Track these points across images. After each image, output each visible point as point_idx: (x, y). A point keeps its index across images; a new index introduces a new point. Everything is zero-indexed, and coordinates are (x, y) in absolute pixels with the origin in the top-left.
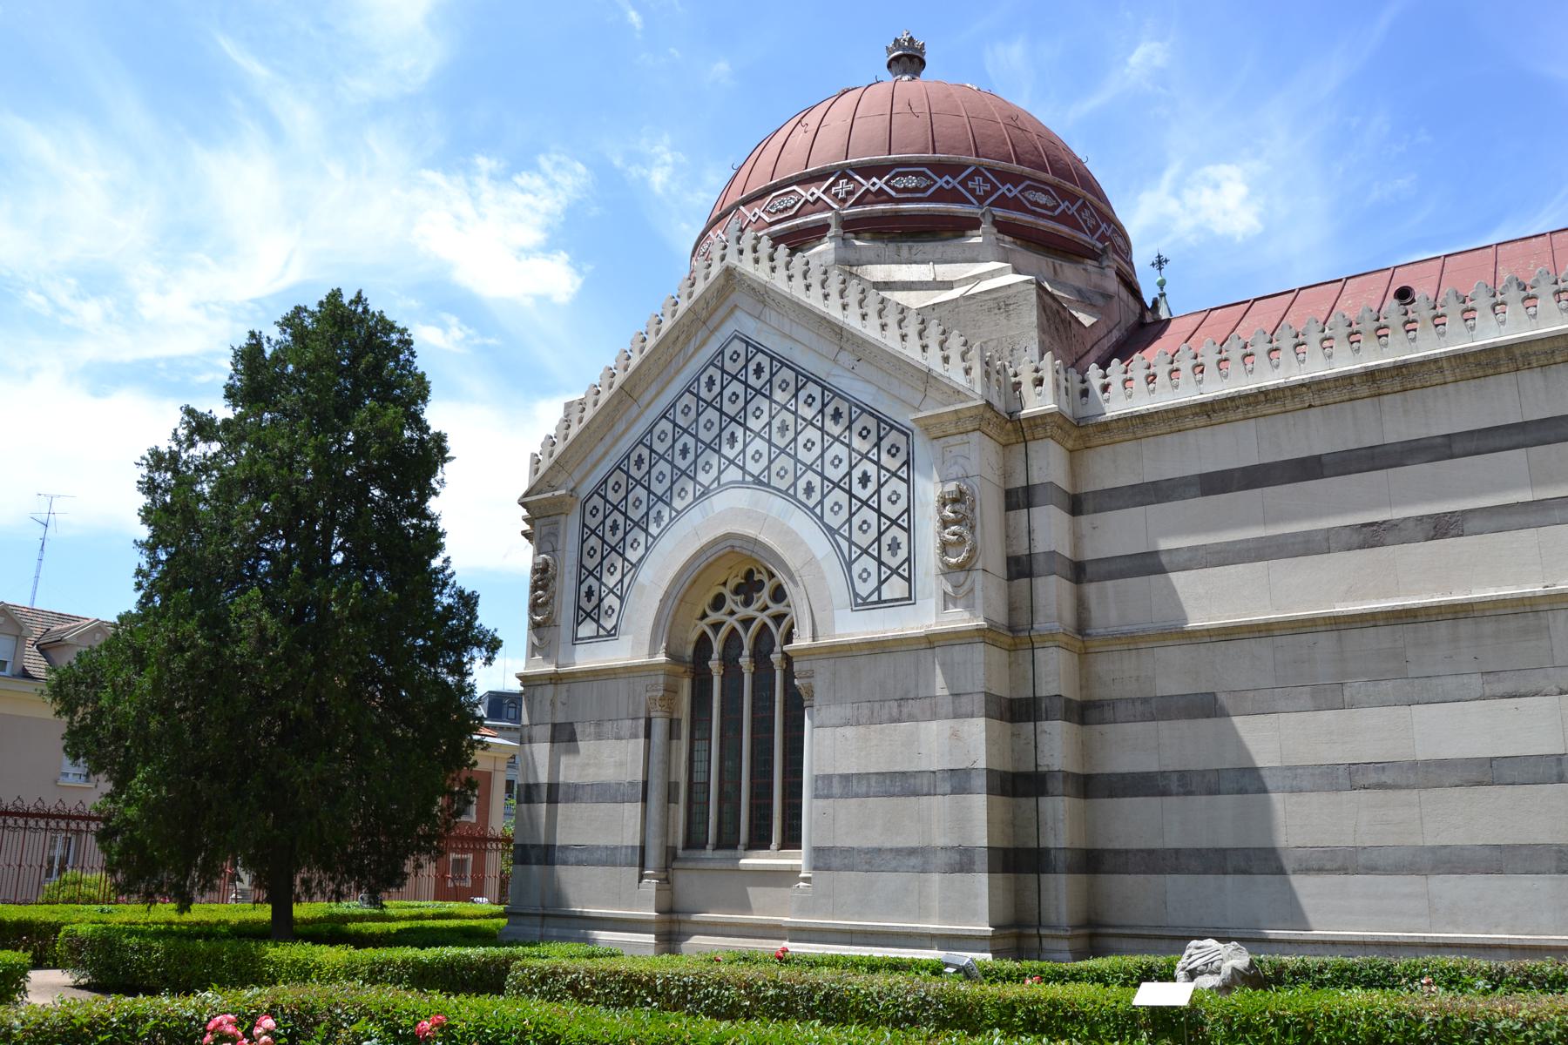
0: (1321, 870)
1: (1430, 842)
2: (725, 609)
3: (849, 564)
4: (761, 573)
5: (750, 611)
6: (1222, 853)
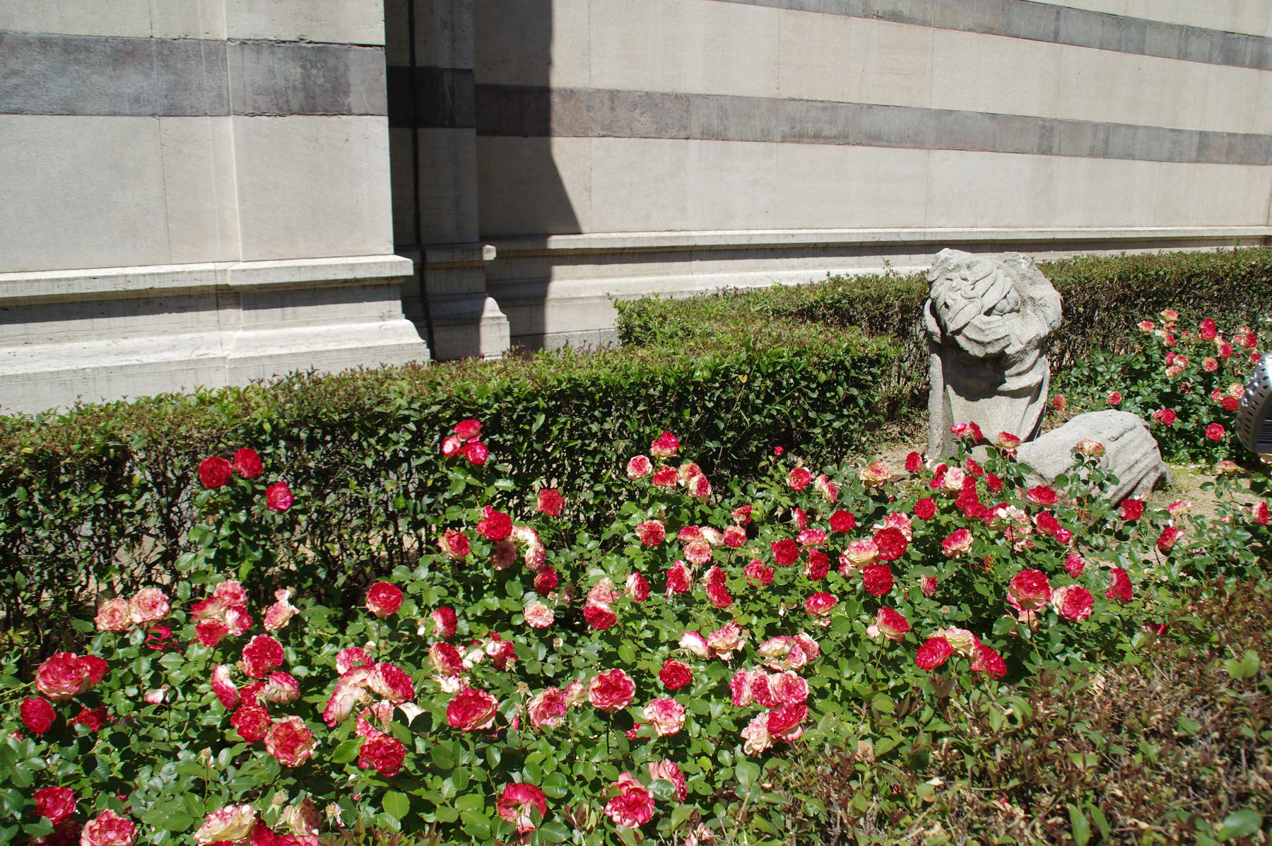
0: (817, 138)
1: (938, 103)
6: (684, 100)
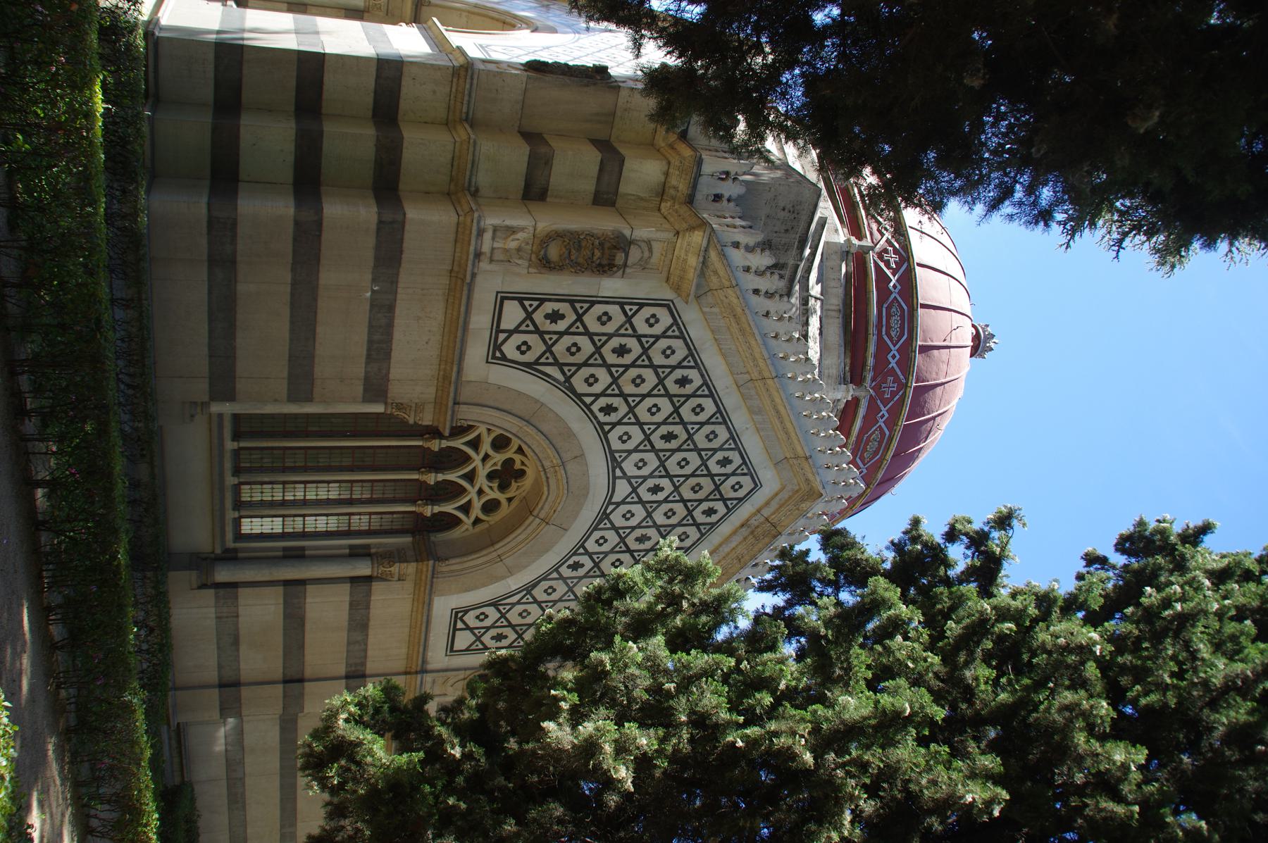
2: (491, 452)
3: (495, 604)
4: (518, 488)
5: (481, 480)
